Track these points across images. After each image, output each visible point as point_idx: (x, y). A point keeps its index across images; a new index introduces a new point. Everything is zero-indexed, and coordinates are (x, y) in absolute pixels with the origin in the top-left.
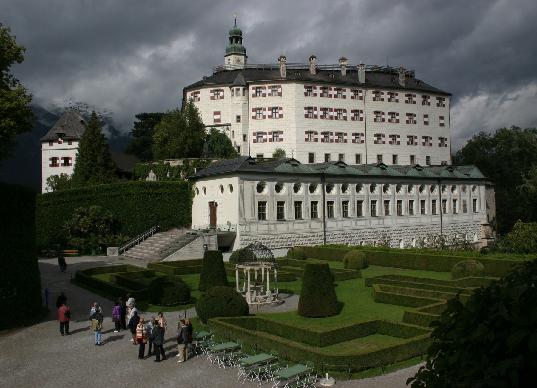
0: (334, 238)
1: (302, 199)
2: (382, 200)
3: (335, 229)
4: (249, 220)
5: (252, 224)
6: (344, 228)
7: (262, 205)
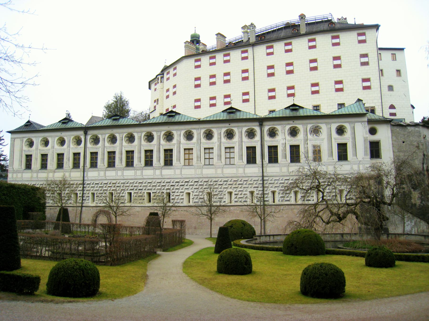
0: (96, 187)
1: (64, 151)
2: (160, 148)
3: (97, 178)
4: (16, 169)
5: (19, 173)
6: (108, 178)
7: (29, 158)
